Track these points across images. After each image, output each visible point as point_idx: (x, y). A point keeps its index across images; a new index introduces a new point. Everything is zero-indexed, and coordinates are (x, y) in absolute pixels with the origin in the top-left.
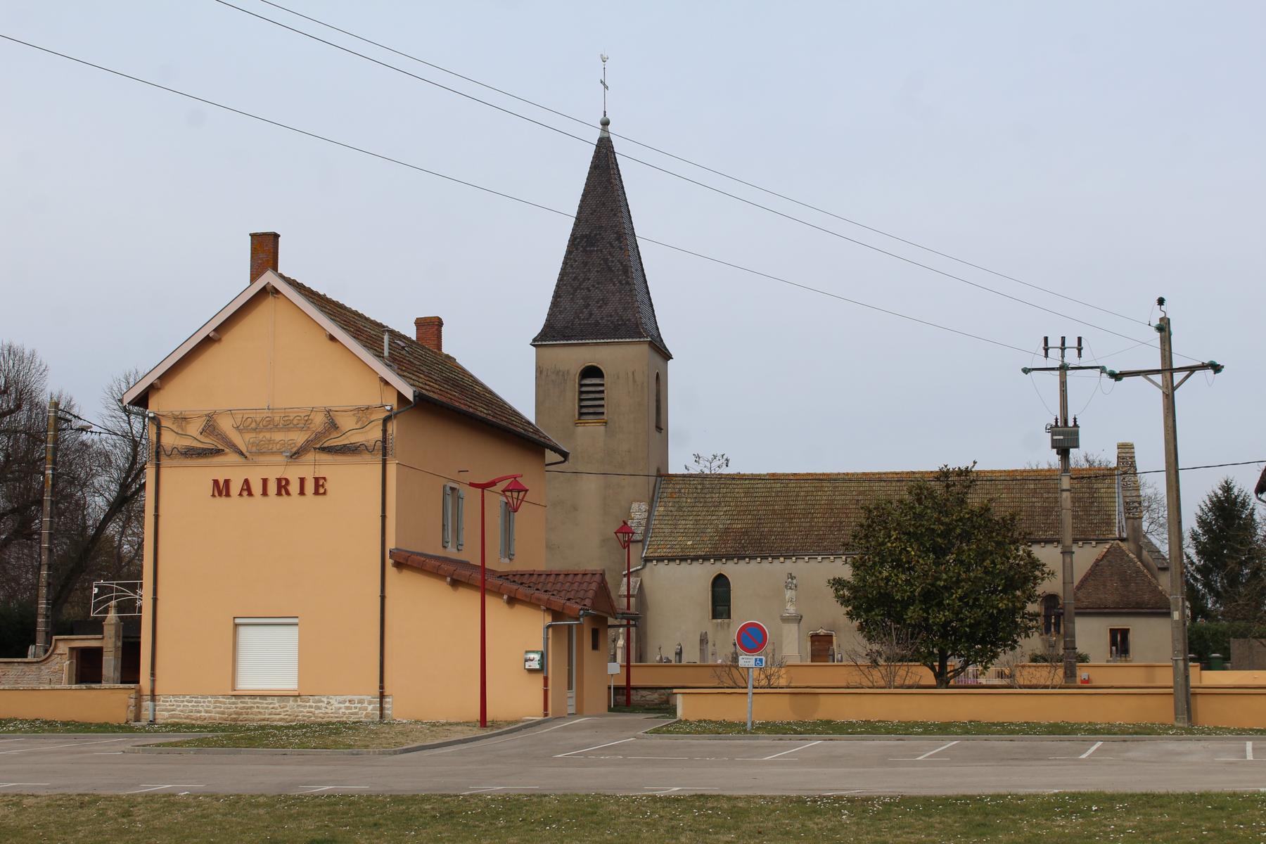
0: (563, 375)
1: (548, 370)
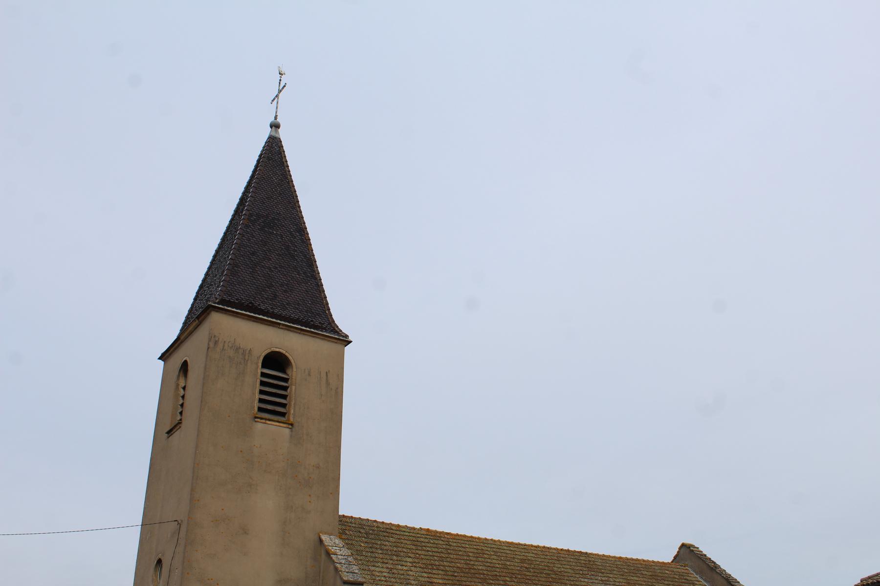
0: (244, 354)
1: (225, 342)
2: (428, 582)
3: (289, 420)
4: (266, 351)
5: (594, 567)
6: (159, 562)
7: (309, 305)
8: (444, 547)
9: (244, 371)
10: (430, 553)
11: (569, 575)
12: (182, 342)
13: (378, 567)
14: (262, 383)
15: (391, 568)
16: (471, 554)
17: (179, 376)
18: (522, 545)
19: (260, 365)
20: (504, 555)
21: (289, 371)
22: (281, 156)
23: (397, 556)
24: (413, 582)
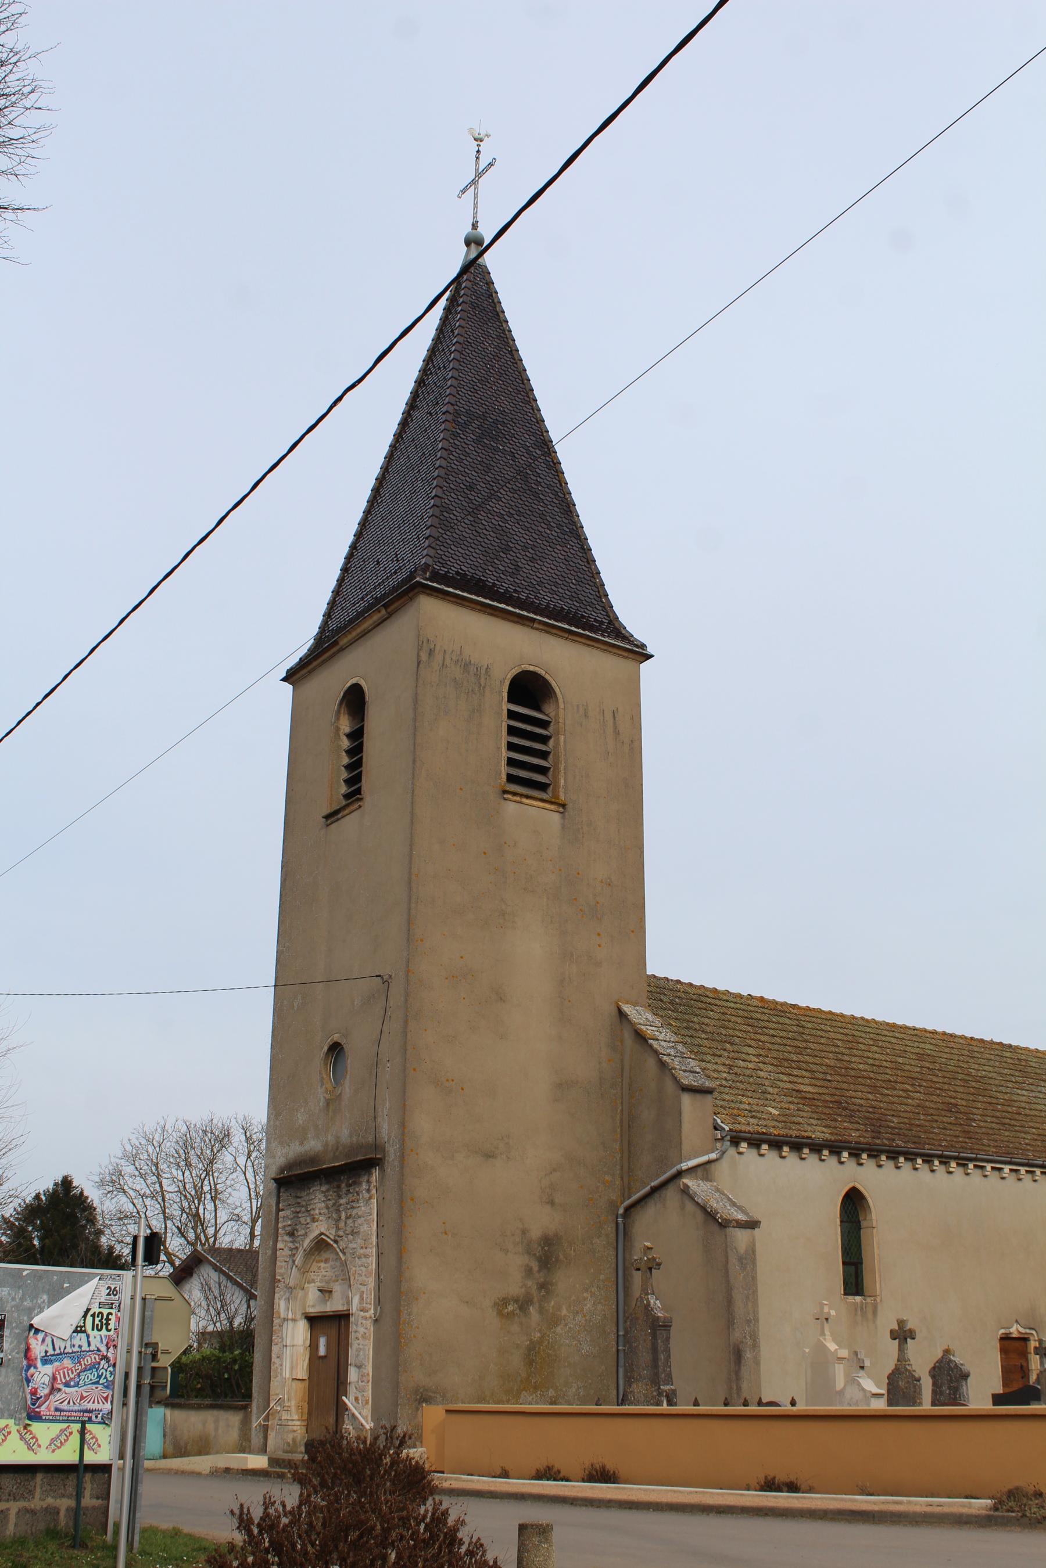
0: (477, 675)
1: (445, 651)
2: (794, 1090)
3: (556, 795)
4: (514, 670)
5: (1029, 1070)
6: (336, 1049)
7: (574, 587)
8: (795, 1028)
9: (480, 706)
10: (779, 1040)
11: (997, 1082)
12: (342, 649)
13: (709, 1062)
14: (512, 731)
15: (729, 1065)
16: (839, 1043)
17: (338, 712)
18: (910, 1028)
19: (505, 695)
20: (889, 1046)
21: (549, 709)
22: (493, 300)
23: (731, 1044)
24: (770, 1090)
